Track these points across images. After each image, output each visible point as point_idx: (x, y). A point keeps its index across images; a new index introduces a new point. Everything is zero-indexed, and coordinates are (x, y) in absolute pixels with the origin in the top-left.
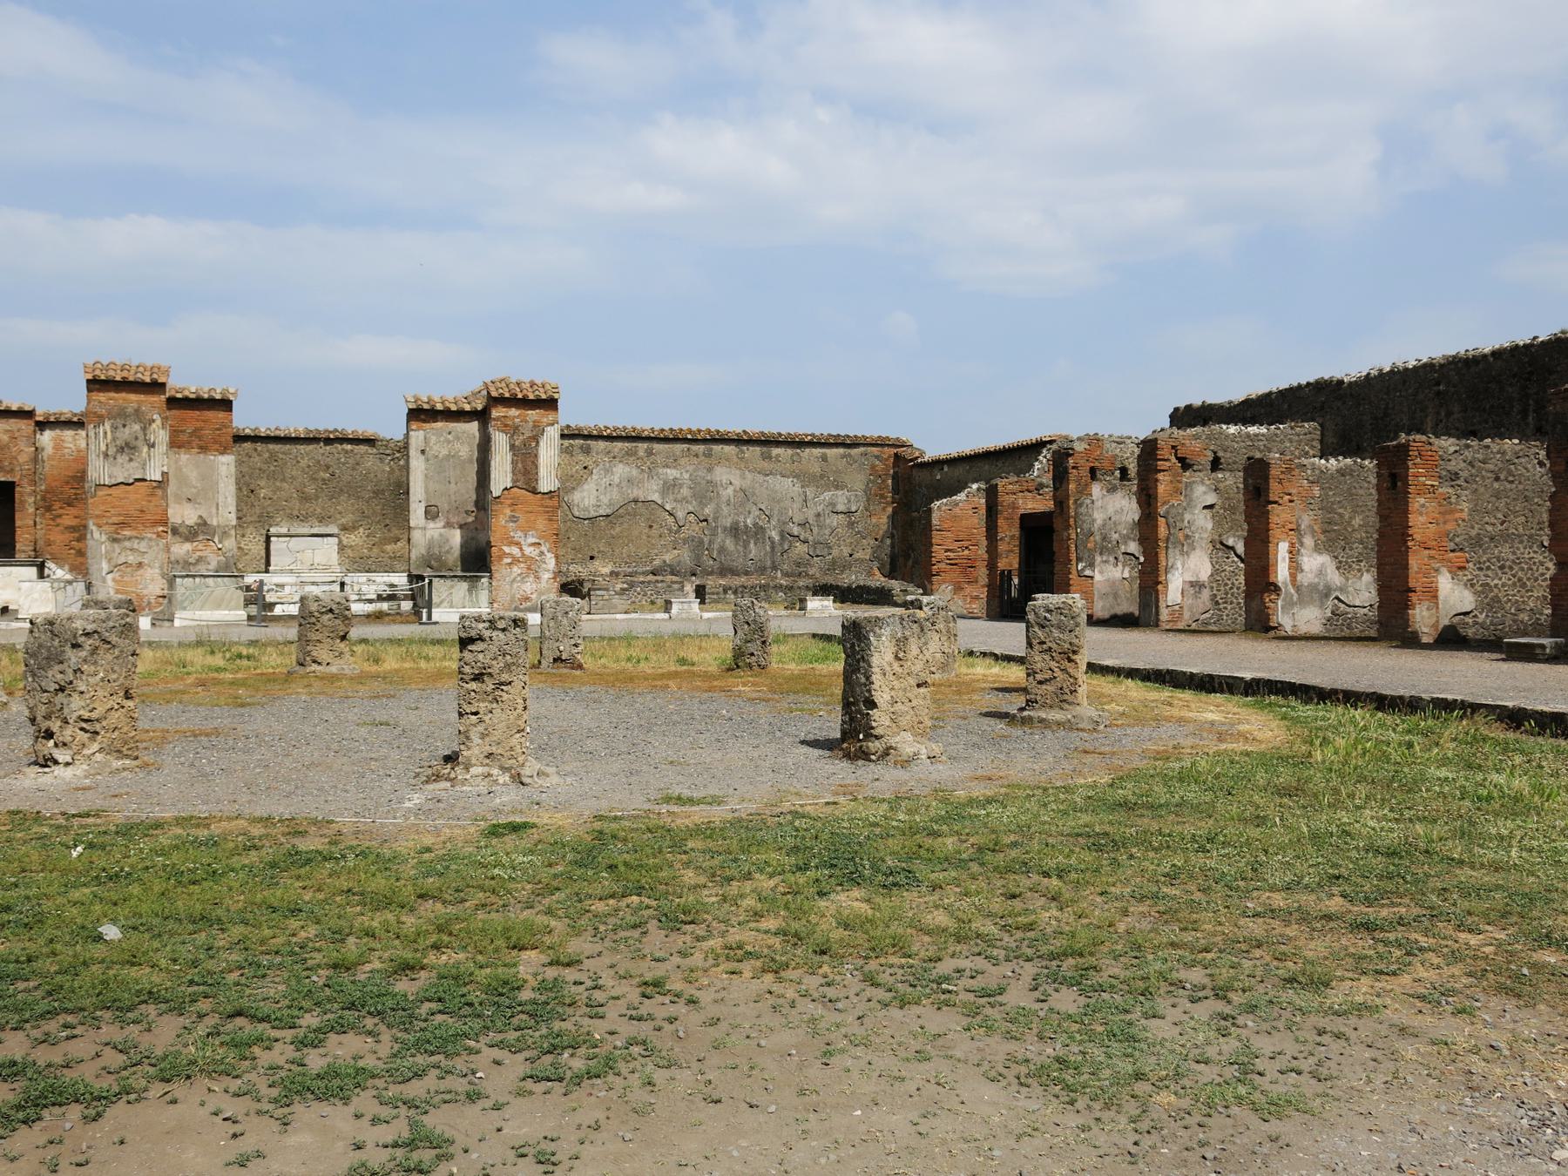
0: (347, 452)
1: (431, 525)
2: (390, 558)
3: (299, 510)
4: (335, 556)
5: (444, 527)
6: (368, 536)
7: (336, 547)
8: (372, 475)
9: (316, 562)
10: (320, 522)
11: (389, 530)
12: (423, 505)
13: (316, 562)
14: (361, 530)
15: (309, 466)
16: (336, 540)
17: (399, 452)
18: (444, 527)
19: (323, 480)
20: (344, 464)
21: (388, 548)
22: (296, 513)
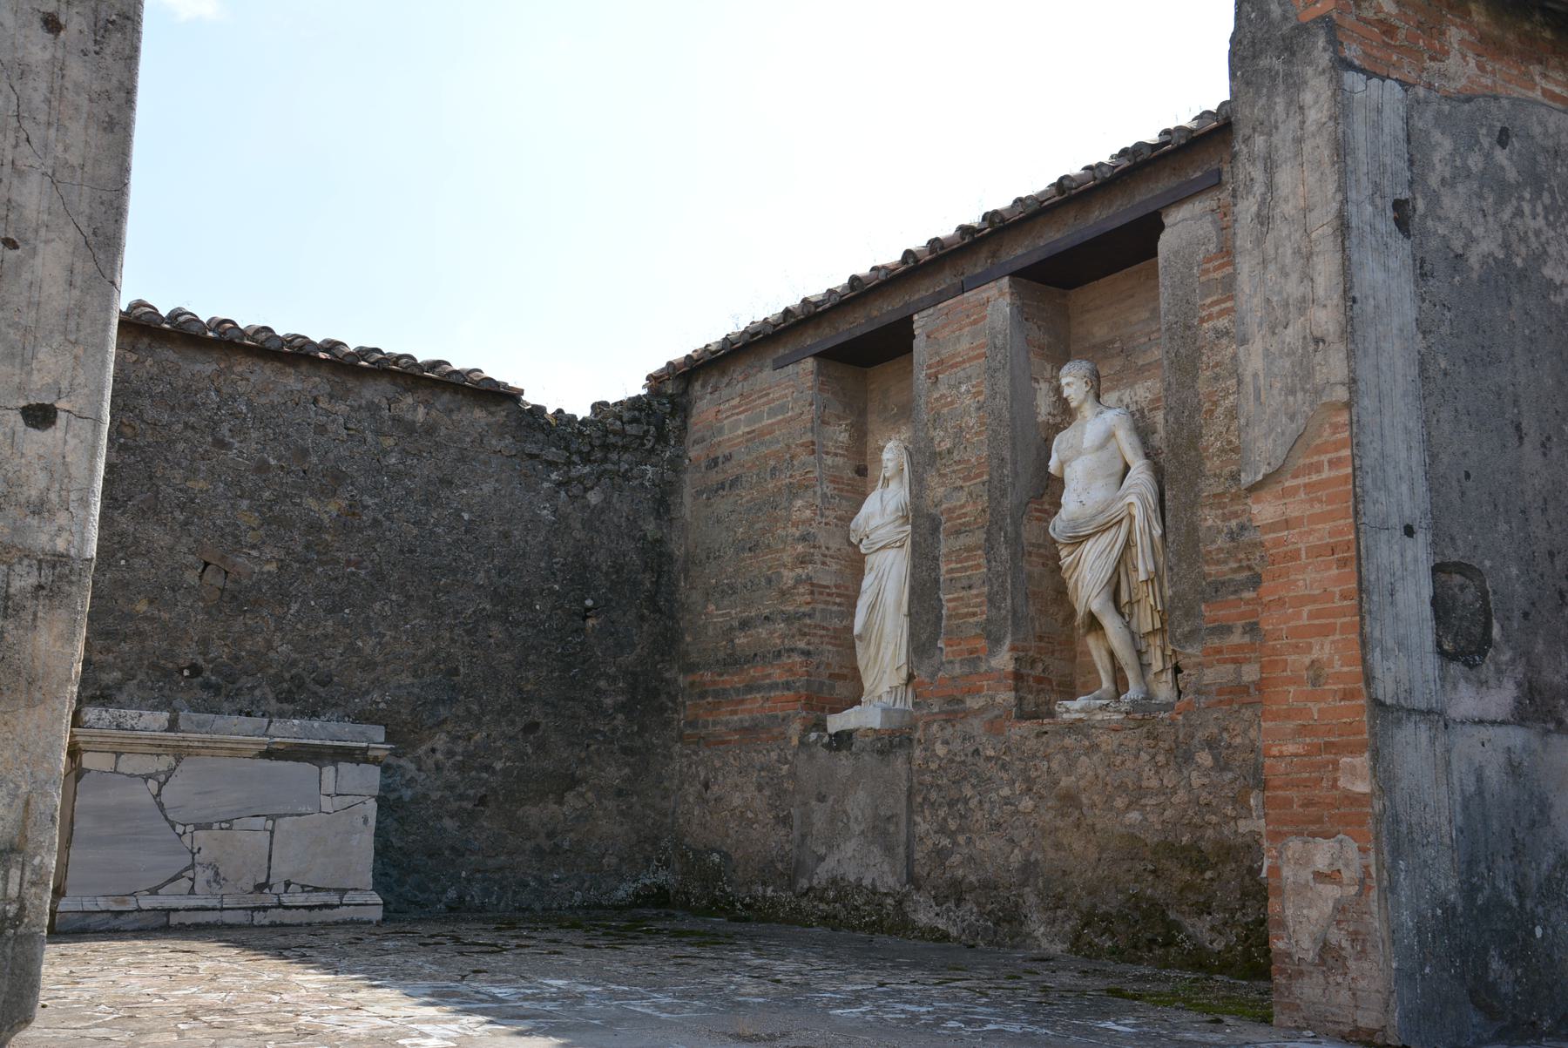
0: (410, 428)
1: (1466, 701)
2: (539, 852)
3: (205, 642)
4: (363, 845)
5: (1520, 717)
6: (461, 768)
7: (371, 807)
8: (494, 530)
9: (281, 870)
10: (287, 697)
11: (541, 747)
12: (1419, 552)
13: (282, 869)
14: (441, 741)
15: (262, 468)
16: (373, 775)
17: (586, 460)
18: (1520, 717)
19: (315, 527)
20: (396, 476)
21: (534, 814)
22: (188, 653)
